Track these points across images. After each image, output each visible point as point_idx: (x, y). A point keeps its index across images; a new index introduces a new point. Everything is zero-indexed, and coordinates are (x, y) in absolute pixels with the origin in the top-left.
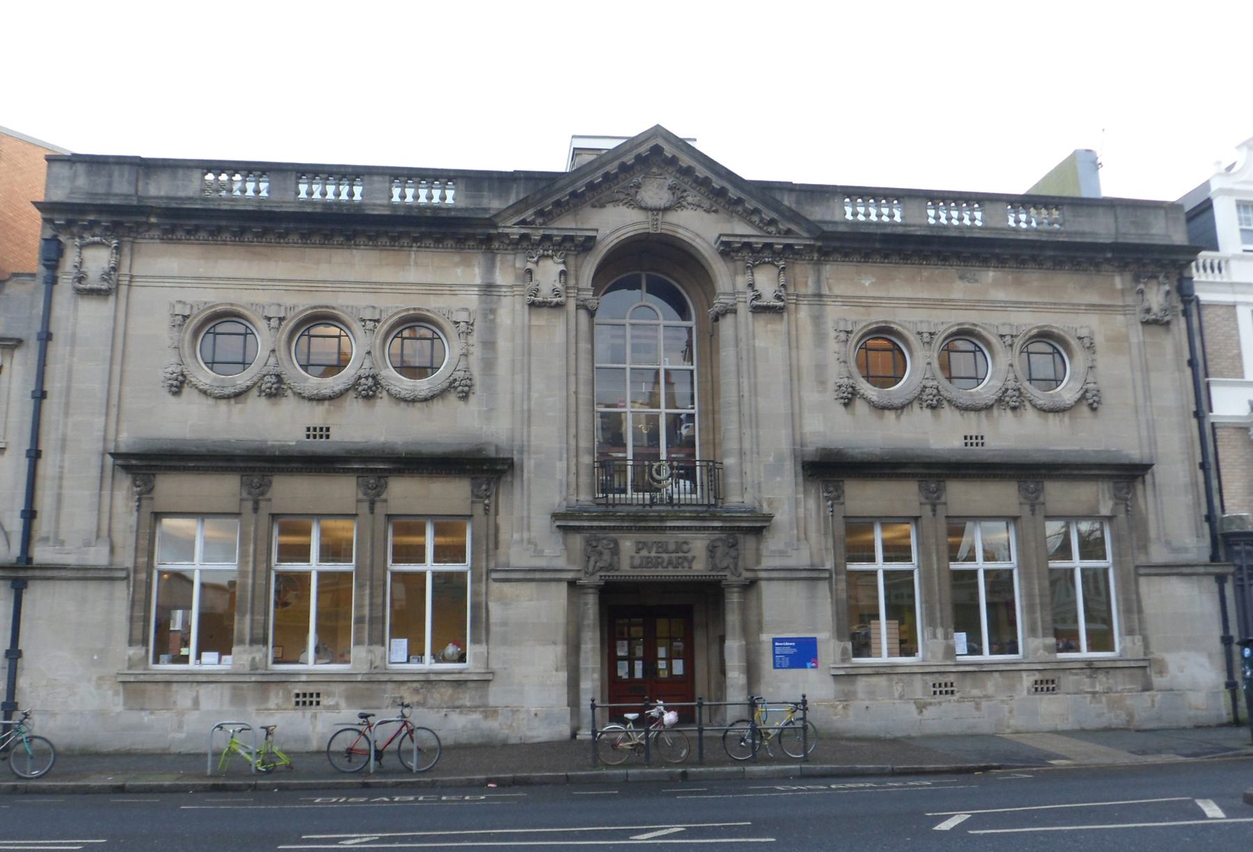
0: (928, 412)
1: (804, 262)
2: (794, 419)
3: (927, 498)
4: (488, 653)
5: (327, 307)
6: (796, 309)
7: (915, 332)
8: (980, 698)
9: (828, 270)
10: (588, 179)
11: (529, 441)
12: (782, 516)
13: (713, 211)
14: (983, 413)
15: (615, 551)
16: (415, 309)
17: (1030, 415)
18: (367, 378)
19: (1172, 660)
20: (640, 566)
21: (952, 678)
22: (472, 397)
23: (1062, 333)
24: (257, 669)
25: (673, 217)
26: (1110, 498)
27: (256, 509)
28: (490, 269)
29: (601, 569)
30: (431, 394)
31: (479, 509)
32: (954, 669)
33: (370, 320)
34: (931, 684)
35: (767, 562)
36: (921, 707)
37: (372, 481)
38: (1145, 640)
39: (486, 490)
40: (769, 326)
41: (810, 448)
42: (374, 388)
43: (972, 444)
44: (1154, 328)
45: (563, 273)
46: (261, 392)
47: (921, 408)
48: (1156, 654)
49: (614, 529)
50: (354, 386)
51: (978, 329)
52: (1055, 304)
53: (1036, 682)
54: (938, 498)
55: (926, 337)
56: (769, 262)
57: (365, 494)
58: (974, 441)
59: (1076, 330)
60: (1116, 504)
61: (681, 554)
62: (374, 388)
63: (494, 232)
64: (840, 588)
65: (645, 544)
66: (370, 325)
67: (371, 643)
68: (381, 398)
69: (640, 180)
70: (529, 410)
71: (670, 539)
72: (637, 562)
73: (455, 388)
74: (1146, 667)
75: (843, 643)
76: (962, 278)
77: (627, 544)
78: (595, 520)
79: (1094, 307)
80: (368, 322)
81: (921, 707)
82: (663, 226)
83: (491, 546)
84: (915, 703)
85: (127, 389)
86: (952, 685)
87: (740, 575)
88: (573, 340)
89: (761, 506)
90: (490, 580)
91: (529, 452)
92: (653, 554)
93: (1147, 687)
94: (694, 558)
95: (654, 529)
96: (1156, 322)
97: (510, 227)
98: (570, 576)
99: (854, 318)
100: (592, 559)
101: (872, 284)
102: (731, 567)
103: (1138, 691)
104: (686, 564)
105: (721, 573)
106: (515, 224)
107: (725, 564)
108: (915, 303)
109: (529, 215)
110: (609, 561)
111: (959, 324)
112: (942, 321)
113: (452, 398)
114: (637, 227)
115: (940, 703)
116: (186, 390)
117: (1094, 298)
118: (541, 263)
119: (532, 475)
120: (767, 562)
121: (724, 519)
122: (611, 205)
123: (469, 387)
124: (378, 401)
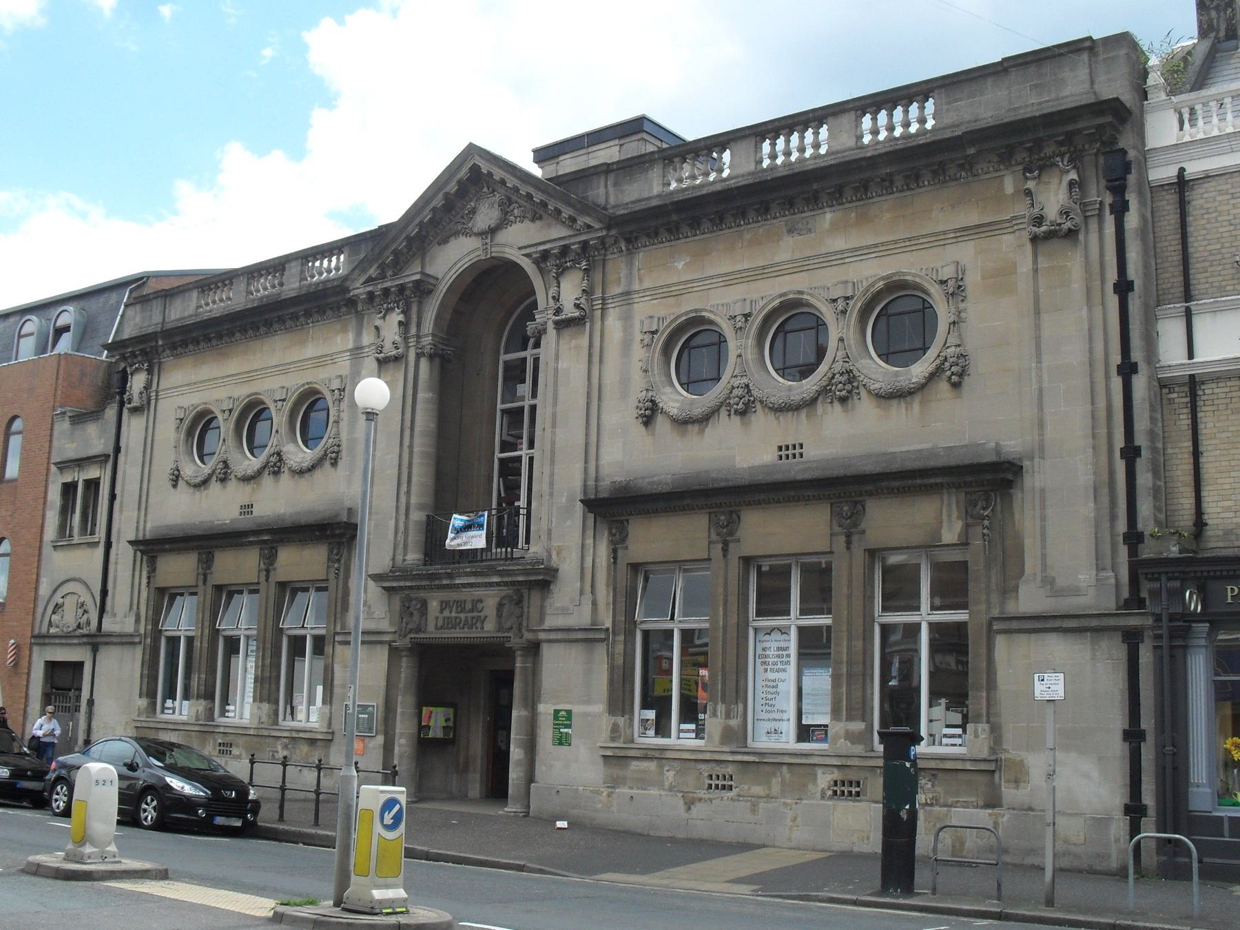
0: (736, 420)
2: (591, 450)
4: (331, 713)
5: (256, 394)
8: (760, 797)
10: (417, 221)
12: (568, 567)
13: (537, 219)
14: (803, 413)
16: (308, 383)
17: (865, 407)
19: (1036, 764)
20: (441, 628)
21: (730, 769)
22: (340, 463)
23: (918, 280)
24: (199, 720)
25: (502, 237)
26: (958, 518)
27: (205, 581)
28: (359, 334)
31: (332, 576)
32: (730, 758)
34: (706, 774)
35: (550, 622)
36: (689, 804)
38: (996, 731)
39: (337, 554)
41: (605, 483)
42: (278, 464)
43: (787, 457)
44: (1055, 244)
46: (217, 477)
47: (729, 415)
48: (1012, 750)
51: (805, 297)
52: (910, 239)
53: (836, 783)
55: (740, 322)
56: (571, 267)
58: (790, 452)
59: (937, 271)
60: (967, 527)
61: (475, 614)
62: (278, 464)
63: (348, 296)
64: (617, 651)
65: (447, 603)
66: (280, 403)
71: (467, 595)
72: (440, 623)
74: (993, 772)
78: (400, 580)
79: (965, 232)
81: (689, 804)
82: (493, 249)
83: (339, 609)
85: (151, 486)
88: (410, 392)
92: (454, 614)
93: (993, 802)
94: (486, 617)
96: (1050, 235)
97: (357, 288)
98: (387, 638)
99: (662, 313)
101: (686, 264)
103: (977, 807)
105: (506, 635)
107: (508, 625)
108: (730, 279)
109: (373, 272)
110: (417, 622)
111: (780, 296)
112: (762, 295)
115: (711, 800)
116: (180, 482)
117: (973, 217)
120: (550, 622)
124: (282, 475)
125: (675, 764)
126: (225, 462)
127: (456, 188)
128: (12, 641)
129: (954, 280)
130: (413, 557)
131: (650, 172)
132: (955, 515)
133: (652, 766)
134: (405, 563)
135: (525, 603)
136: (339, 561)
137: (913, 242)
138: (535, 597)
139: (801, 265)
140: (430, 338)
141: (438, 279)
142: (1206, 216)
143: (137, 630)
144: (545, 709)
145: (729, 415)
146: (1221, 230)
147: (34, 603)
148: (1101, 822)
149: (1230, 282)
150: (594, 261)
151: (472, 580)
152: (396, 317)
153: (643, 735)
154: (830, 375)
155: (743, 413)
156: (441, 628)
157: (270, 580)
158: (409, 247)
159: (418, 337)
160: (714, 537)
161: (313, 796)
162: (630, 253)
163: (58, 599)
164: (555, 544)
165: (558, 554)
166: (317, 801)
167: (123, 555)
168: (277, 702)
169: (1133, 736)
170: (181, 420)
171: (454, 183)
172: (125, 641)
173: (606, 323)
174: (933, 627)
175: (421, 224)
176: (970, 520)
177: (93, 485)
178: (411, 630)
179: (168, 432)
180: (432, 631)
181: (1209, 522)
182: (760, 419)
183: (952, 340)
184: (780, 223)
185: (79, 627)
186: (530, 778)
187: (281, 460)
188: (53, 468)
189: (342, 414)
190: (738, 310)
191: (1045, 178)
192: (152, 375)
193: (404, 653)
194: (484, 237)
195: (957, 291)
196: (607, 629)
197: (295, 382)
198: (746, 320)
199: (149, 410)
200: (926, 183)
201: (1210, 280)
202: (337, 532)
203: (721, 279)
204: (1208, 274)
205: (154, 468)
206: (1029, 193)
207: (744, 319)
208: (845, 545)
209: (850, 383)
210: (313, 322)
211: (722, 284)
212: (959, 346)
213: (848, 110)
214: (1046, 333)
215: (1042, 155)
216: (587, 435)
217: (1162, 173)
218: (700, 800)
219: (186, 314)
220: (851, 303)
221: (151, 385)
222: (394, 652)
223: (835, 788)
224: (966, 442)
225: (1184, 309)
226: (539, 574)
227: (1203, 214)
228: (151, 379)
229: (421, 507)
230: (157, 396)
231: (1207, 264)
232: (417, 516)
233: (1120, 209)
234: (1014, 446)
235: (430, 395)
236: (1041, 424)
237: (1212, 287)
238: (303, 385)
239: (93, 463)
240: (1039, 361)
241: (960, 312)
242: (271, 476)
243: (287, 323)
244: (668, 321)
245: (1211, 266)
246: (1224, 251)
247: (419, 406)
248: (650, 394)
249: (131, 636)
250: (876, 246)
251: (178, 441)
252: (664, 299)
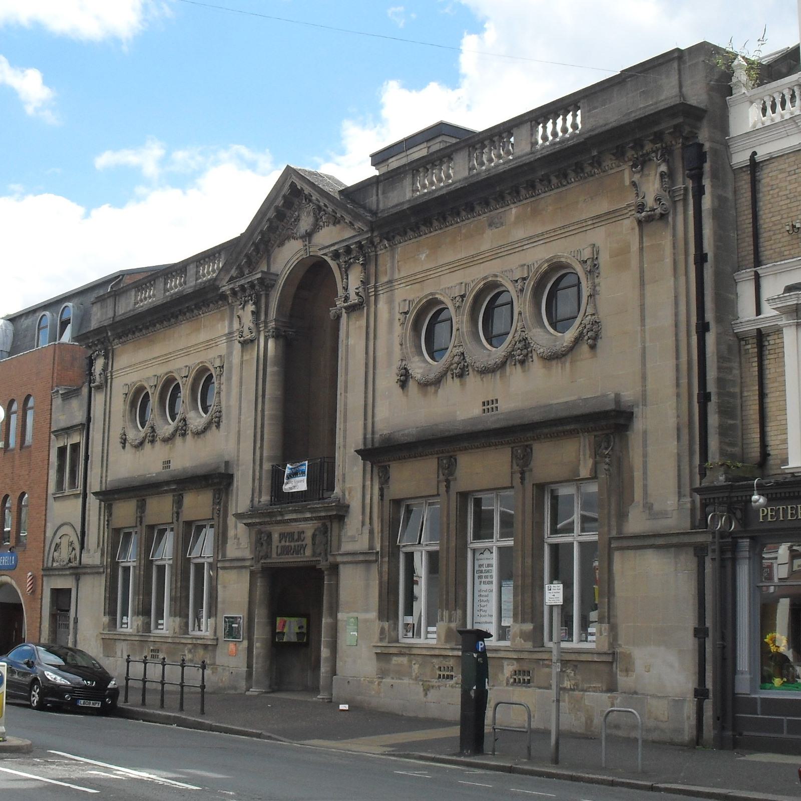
0: (457, 381)
2: (369, 409)
4: (216, 624)
17: (536, 366)
19: (641, 655)
23: (569, 261)
24: (139, 632)
34: (437, 667)
35: (347, 547)
36: (426, 691)
38: (613, 629)
42: (184, 428)
47: (453, 378)
48: (624, 647)
60: (596, 464)
61: (300, 543)
62: (184, 428)
74: (612, 663)
75: (381, 623)
79: (599, 219)
81: (426, 691)
87: (327, 560)
92: (287, 544)
93: (612, 688)
94: (306, 545)
96: (650, 219)
97: (224, 286)
98: (248, 563)
101: (427, 256)
103: (602, 691)
107: (318, 551)
108: (455, 267)
112: (472, 279)
116: (127, 444)
120: (347, 547)
124: (187, 436)
125: (419, 659)
126: (152, 427)
127: (283, 201)
128: (30, 574)
129: (591, 260)
130: (265, 498)
131: (405, 181)
132: (588, 456)
133: (404, 660)
134: (260, 504)
137: (566, 230)
138: (335, 526)
139: (496, 254)
140: (274, 323)
141: (278, 275)
142: (771, 192)
143: (102, 562)
145: (453, 378)
146: (782, 203)
147: (44, 543)
148: (678, 703)
149: (787, 248)
150: (369, 256)
151: (294, 516)
152: (251, 307)
153: (405, 637)
154: (513, 343)
155: (461, 376)
156: (280, 555)
157: (180, 520)
158: (257, 250)
159: (266, 323)
160: (441, 477)
161: (200, 690)
162: (393, 247)
163: (57, 540)
164: (348, 485)
165: (349, 493)
166: (203, 692)
167: (93, 503)
169: (700, 633)
170: (126, 394)
171: (280, 198)
172: (94, 571)
173: (378, 306)
174: (581, 544)
175: (261, 232)
176: (598, 458)
177: (75, 447)
178: (262, 556)
179: (119, 405)
180: (276, 559)
181: (772, 453)
182: (472, 379)
183: (590, 311)
185: (70, 561)
186: (334, 672)
187: (186, 425)
188: (53, 436)
189: (222, 387)
190: (457, 292)
191: (646, 172)
192: (108, 360)
195: (593, 269)
196: (378, 553)
197: (194, 361)
198: (463, 300)
199: (106, 387)
200: (573, 180)
201: (773, 247)
202: (216, 481)
204: (772, 242)
205: (111, 433)
206: (634, 184)
208: (520, 480)
209: (526, 348)
210: (203, 314)
211: (448, 271)
212: (594, 314)
213: (526, 122)
214: (648, 301)
215: (645, 151)
216: (366, 397)
217: (740, 158)
218: (433, 687)
219: (129, 309)
220: (527, 282)
221: (108, 368)
222: (252, 574)
223: (515, 677)
224: (599, 394)
225: (753, 273)
226: (332, 510)
227: (769, 191)
228: (108, 363)
229: (270, 459)
230: (112, 376)
231: (771, 233)
232: (267, 466)
233: (699, 192)
234: (629, 395)
235: (275, 369)
236: (644, 377)
237: (775, 252)
239: (76, 431)
240: (643, 324)
241: (595, 286)
242: (150, 444)
244: (415, 302)
245: (774, 234)
246: (783, 221)
247: (268, 378)
248: (404, 363)
249: (98, 567)
250: (542, 234)
251: (125, 411)
252: (414, 285)
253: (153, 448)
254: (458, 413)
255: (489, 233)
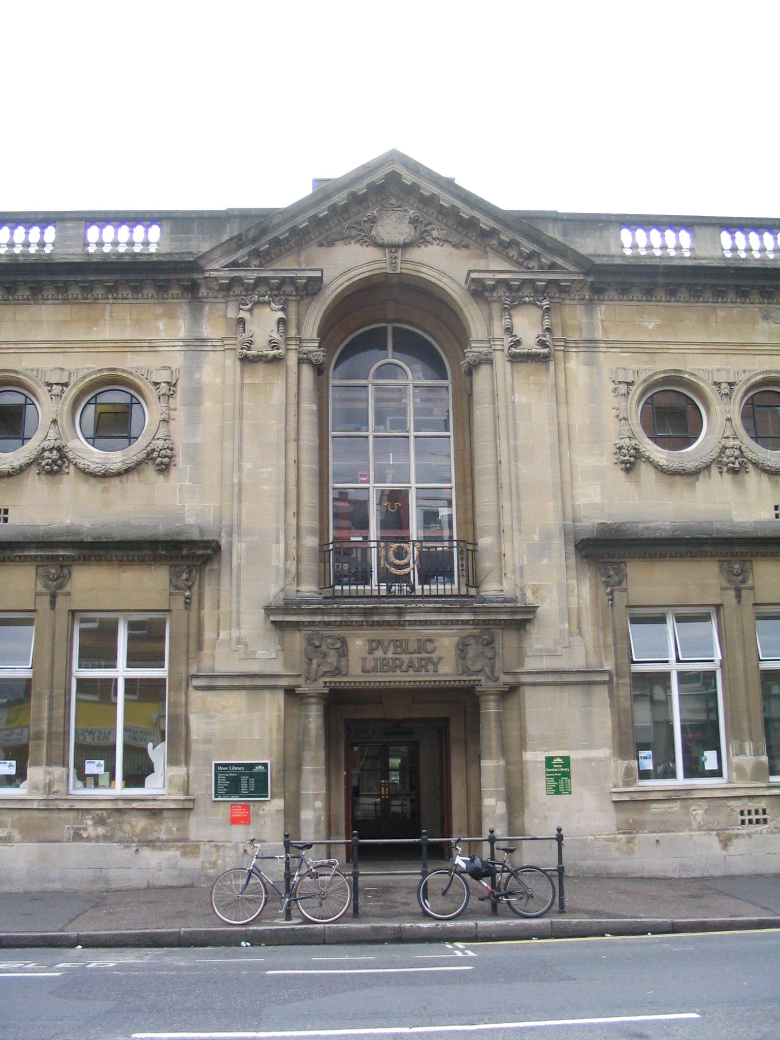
0: (727, 477)
1: (575, 302)
3: (729, 582)
4: (188, 775)
6: (565, 357)
7: (711, 381)
9: (602, 311)
10: (311, 213)
11: (239, 520)
13: (464, 246)
15: (343, 652)
18: (51, 450)
20: (374, 670)
21: (762, 804)
29: (325, 674)
30: (125, 467)
31: (179, 603)
32: (767, 793)
33: (57, 384)
34: (739, 811)
35: (531, 664)
36: (725, 843)
37: (53, 571)
39: (187, 580)
40: (531, 377)
45: (281, 321)
47: (721, 473)
49: (340, 624)
50: (35, 461)
54: (744, 581)
55: (725, 389)
56: (530, 303)
57: (46, 586)
61: (423, 655)
62: (59, 462)
64: (621, 693)
65: (379, 642)
66: (57, 389)
67: (49, 763)
68: (68, 473)
69: (375, 212)
70: (240, 484)
71: (411, 635)
72: (370, 665)
73: (154, 459)
75: (626, 762)
76: (766, 318)
77: (358, 644)
80: (54, 386)
81: (725, 843)
83: (193, 647)
84: (718, 835)
86: (764, 812)
87: (497, 680)
88: (293, 399)
89: (524, 594)
90: (191, 688)
91: (239, 534)
94: (440, 659)
95: (389, 624)
99: (635, 367)
100: (315, 662)
101: (659, 327)
102: (487, 670)
104: (430, 667)
106: (225, 267)
107: (477, 667)
109: (240, 255)
110: (335, 664)
111: (763, 373)
112: (745, 368)
113: (150, 471)
114: (372, 267)
115: (749, 835)
118: (256, 311)
119: (243, 562)
120: (531, 664)
121: (474, 611)
122: (341, 243)
123: (170, 457)
125: (704, 805)
133: (676, 807)
135: (498, 644)
136: (190, 588)
144: (534, 757)
165: (534, 593)
168: (68, 766)
178: (326, 672)
184: (754, 309)
193: (313, 700)
194: (393, 250)
203: (699, 347)
207: (728, 387)
211: (699, 351)
218: (737, 836)
238: (101, 370)
243: (70, 292)
252: (636, 354)
253: (638, 482)
254: (734, 513)
255: (762, 325)
